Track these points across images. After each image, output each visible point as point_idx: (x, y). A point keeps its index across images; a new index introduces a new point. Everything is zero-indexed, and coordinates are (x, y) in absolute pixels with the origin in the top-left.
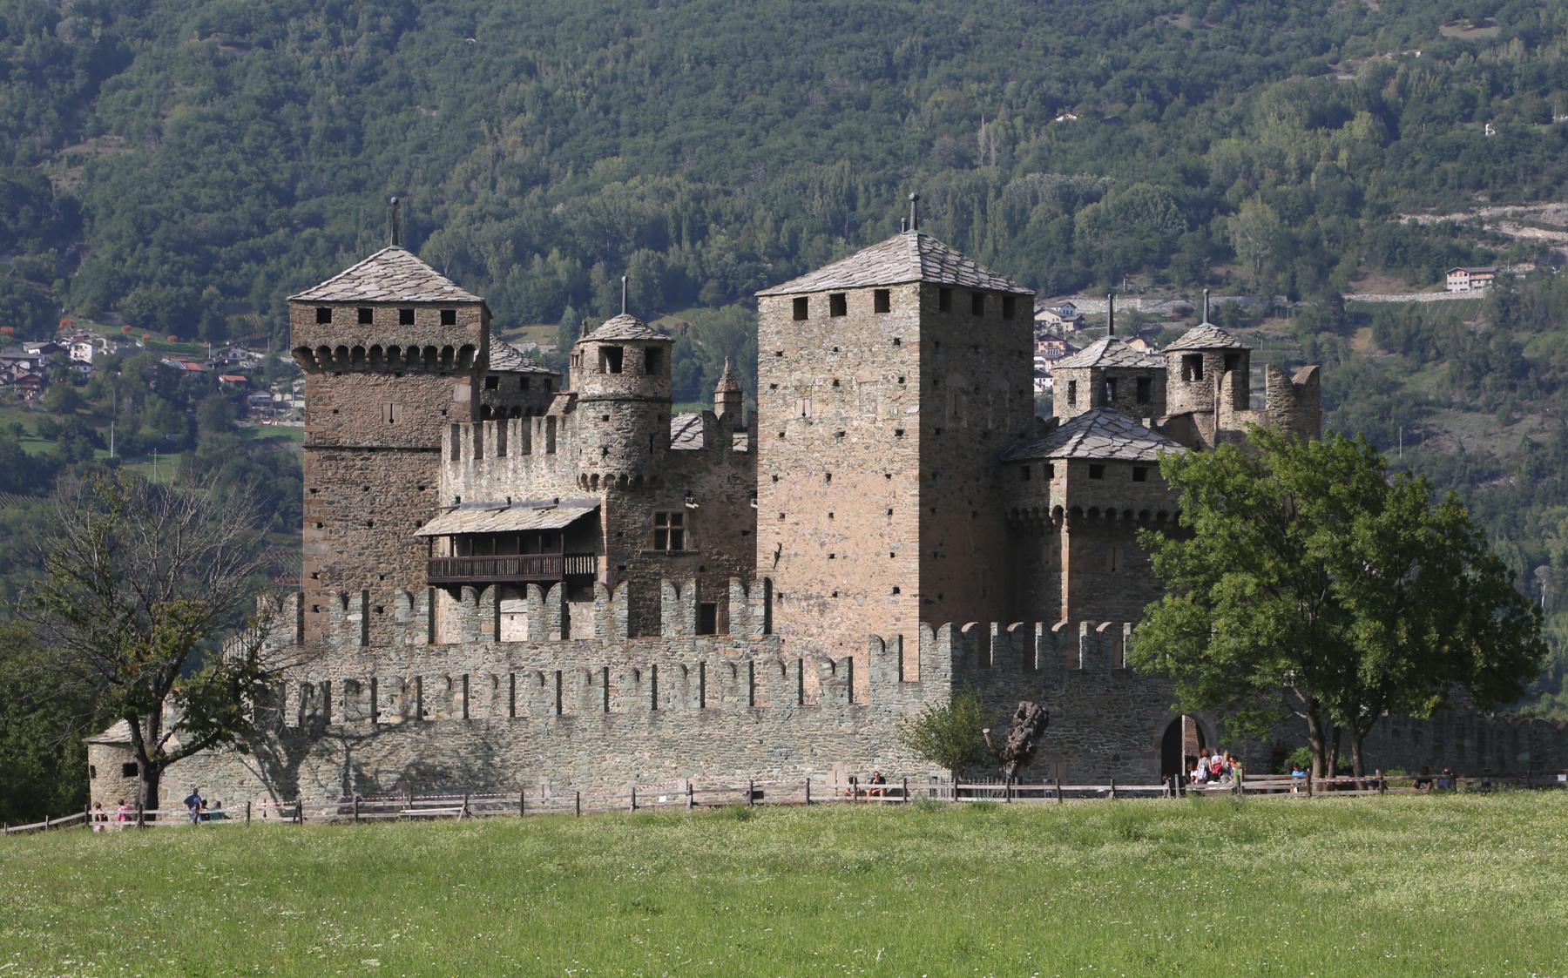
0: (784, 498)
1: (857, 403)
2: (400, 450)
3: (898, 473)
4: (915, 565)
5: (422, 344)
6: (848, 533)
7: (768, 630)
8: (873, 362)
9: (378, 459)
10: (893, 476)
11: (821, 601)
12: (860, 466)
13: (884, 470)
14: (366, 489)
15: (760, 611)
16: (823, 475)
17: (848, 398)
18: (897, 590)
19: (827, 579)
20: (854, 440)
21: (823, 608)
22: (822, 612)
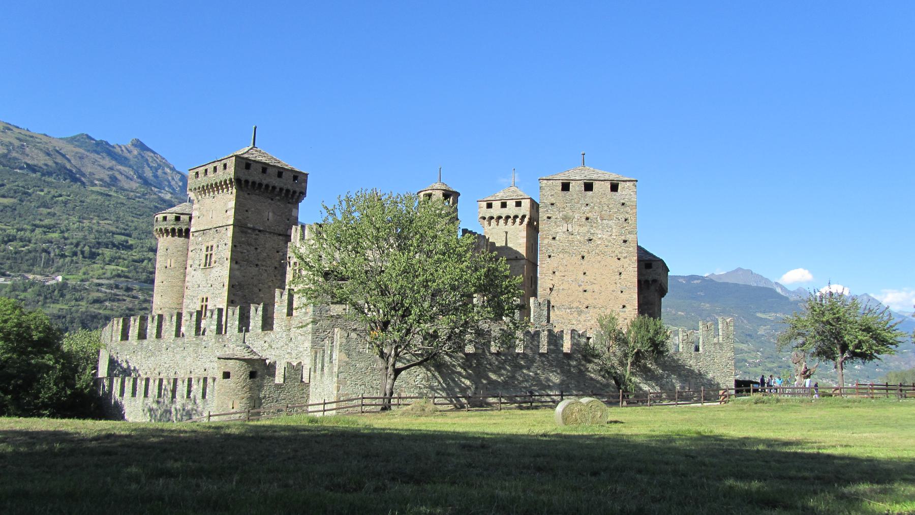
0: (556, 265)
1: (601, 227)
2: (270, 233)
3: (625, 258)
4: (636, 296)
5: (285, 187)
6: (595, 282)
7: (548, 321)
8: (610, 211)
9: (262, 236)
10: (622, 259)
11: (579, 310)
12: (602, 253)
13: (617, 256)
14: (256, 249)
15: (545, 313)
16: (580, 257)
17: (594, 225)
18: (624, 307)
19: (582, 301)
20: (599, 243)
21: (580, 313)
22: (579, 315)
